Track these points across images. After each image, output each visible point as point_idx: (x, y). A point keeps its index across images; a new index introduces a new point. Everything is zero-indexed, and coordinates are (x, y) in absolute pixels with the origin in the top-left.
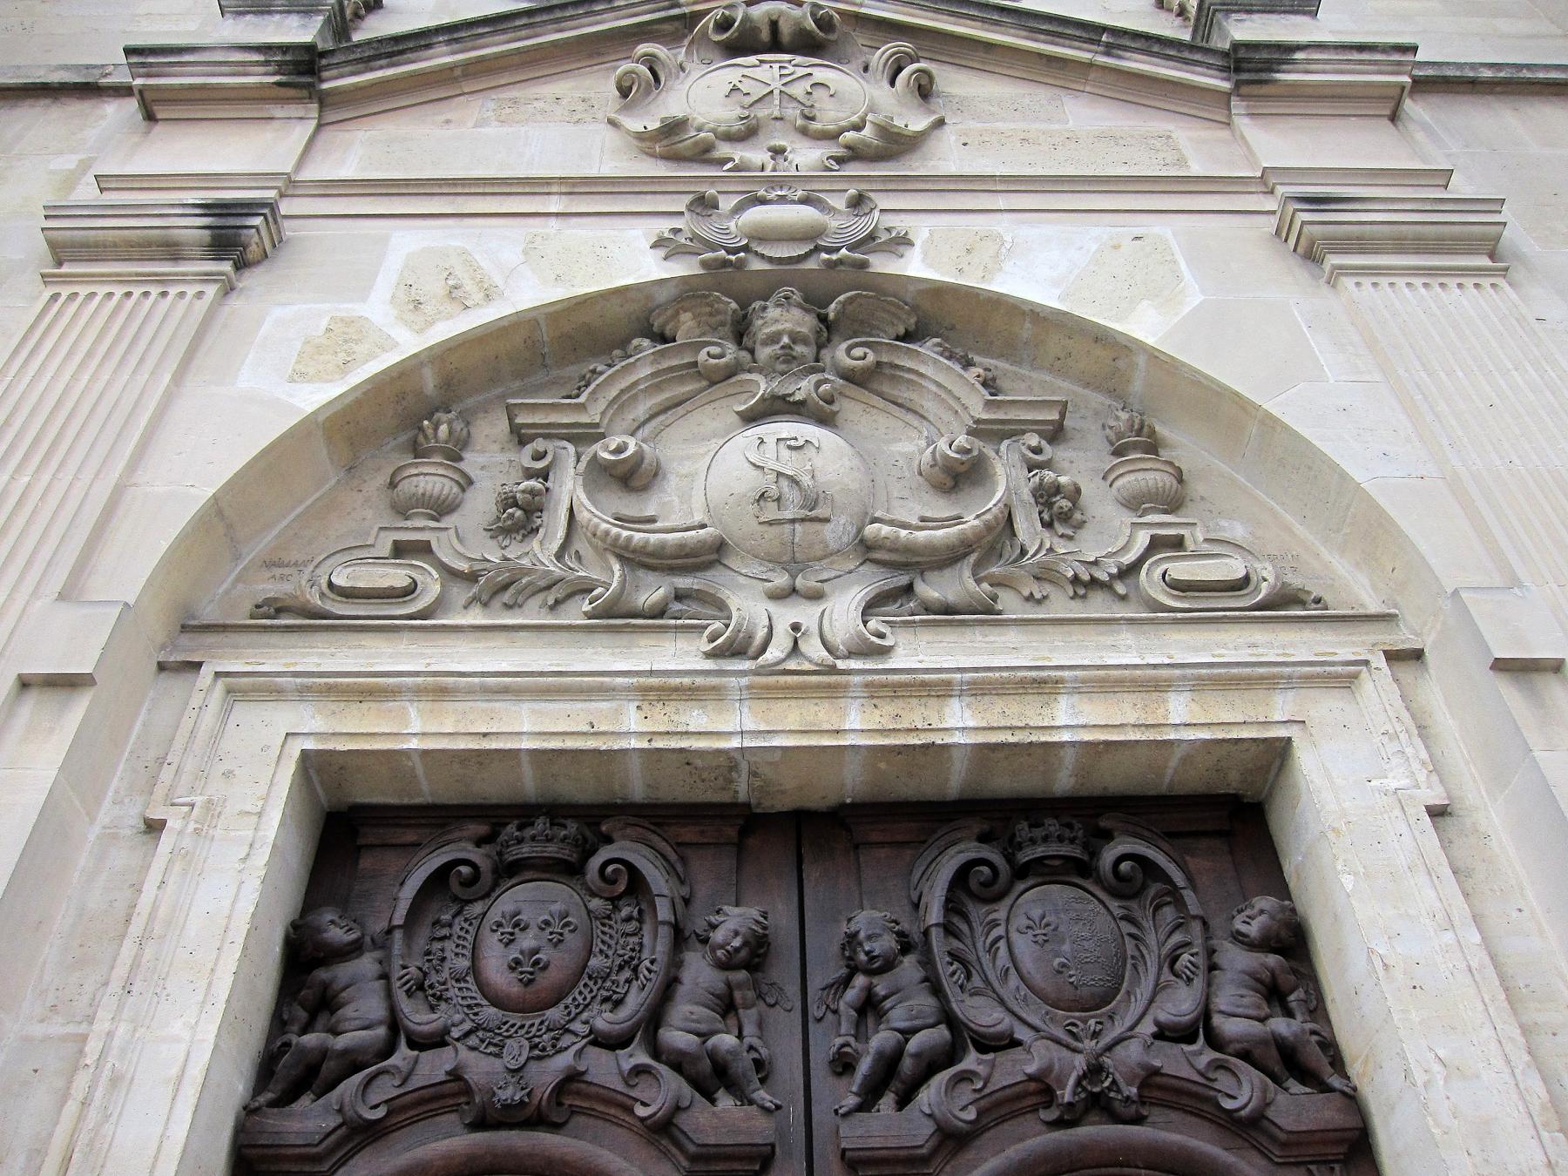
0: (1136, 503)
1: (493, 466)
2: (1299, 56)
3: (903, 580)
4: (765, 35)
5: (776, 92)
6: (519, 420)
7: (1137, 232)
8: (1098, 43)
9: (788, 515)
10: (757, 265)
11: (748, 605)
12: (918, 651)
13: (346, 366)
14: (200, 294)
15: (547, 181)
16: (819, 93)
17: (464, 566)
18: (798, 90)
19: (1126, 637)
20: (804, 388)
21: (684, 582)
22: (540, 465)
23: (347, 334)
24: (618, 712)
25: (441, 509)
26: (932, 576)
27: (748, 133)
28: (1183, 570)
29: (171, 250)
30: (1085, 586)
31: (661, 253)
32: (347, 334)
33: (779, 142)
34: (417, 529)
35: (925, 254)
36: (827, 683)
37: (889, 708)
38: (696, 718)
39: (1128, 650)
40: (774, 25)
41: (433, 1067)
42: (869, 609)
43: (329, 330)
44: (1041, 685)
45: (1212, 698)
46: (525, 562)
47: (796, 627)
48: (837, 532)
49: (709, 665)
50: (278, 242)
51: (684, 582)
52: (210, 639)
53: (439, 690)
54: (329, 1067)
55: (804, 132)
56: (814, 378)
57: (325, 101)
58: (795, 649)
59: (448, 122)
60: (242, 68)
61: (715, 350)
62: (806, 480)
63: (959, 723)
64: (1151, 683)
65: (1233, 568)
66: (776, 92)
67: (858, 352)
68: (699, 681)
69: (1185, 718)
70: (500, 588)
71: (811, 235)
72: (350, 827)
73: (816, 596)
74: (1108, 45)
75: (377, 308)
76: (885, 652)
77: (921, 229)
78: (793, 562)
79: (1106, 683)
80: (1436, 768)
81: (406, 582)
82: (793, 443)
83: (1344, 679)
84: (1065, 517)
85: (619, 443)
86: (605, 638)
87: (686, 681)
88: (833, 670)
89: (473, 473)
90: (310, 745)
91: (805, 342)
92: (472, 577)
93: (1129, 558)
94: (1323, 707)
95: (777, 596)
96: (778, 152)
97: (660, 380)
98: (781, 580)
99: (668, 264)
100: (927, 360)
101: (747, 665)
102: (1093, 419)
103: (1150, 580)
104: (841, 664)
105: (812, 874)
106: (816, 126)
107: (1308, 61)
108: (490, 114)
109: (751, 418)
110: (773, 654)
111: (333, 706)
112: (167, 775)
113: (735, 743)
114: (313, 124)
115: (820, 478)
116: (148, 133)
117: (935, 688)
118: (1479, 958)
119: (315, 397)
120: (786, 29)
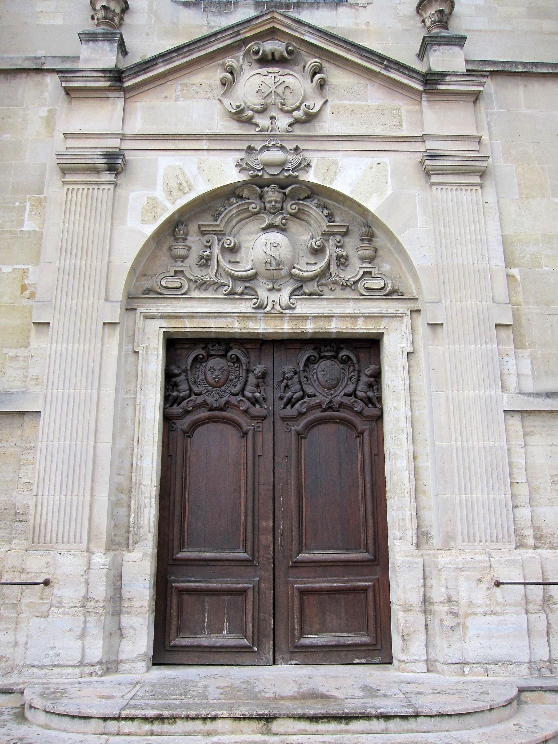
0: (363, 259)
1: (195, 241)
2: (448, 78)
3: (300, 284)
4: (270, 57)
5: (273, 92)
6: (202, 229)
7: (379, 160)
8: (383, 64)
9: (272, 268)
10: (266, 176)
11: (263, 294)
12: (302, 307)
13: (155, 219)
14: (109, 189)
15: (202, 135)
16: (288, 92)
17: (193, 278)
18: (280, 90)
19: (352, 304)
20: (278, 220)
21: (247, 284)
22: (208, 244)
23: (153, 205)
24: (233, 322)
25: (184, 258)
26: (308, 284)
27: (263, 111)
28: (370, 284)
29: (96, 170)
30: (344, 287)
31: (238, 169)
32: (153, 205)
33: (274, 114)
34: (179, 266)
35: (315, 171)
36: (280, 316)
37: (294, 322)
38: (251, 324)
39: (351, 308)
40: (273, 54)
41: (200, 399)
42: (292, 294)
43: (148, 203)
44: (329, 317)
45: (368, 321)
46: (207, 277)
47: (274, 301)
48: (284, 272)
49: (253, 311)
50: (125, 163)
51: (247, 284)
52: (136, 301)
53: (192, 316)
54: (179, 400)
55: (282, 110)
56: (280, 217)
57: (126, 90)
58: (273, 307)
59: (166, 97)
60: (96, 79)
61: (254, 206)
62: (277, 258)
64: (354, 317)
65: (381, 284)
66: (273, 92)
67: (293, 207)
68: (251, 315)
69: (361, 327)
70: (203, 285)
71: (281, 164)
72: (174, 344)
73: (279, 290)
74: (386, 66)
75: (159, 193)
76: (294, 308)
77: (314, 158)
78: (273, 280)
79: (344, 317)
80: (413, 342)
81: (179, 285)
82: (274, 245)
83: (399, 317)
84: (343, 264)
85: (230, 241)
86: (228, 301)
87: (248, 315)
88: (282, 313)
89: (191, 245)
90: (165, 330)
91: (279, 202)
92: (196, 281)
93: (356, 279)
94: (394, 324)
95: (270, 290)
96: (273, 118)
97: (239, 213)
98: (271, 286)
99: (240, 174)
100: (312, 209)
101: (262, 311)
103: (360, 285)
104: (284, 311)
105: (276, 355)
106: (286, 108)
107: (450, 80)
108: (179, 93)
109: (264, 230)
110: (268, 309)
111: (168, 320)
112: (136, 340)
113: (259, 331)
114: (123, 99)
115: (281, 256)
117: (304, 317)
118: (407, 387)
119: (150, 229)
120: (277, 56)
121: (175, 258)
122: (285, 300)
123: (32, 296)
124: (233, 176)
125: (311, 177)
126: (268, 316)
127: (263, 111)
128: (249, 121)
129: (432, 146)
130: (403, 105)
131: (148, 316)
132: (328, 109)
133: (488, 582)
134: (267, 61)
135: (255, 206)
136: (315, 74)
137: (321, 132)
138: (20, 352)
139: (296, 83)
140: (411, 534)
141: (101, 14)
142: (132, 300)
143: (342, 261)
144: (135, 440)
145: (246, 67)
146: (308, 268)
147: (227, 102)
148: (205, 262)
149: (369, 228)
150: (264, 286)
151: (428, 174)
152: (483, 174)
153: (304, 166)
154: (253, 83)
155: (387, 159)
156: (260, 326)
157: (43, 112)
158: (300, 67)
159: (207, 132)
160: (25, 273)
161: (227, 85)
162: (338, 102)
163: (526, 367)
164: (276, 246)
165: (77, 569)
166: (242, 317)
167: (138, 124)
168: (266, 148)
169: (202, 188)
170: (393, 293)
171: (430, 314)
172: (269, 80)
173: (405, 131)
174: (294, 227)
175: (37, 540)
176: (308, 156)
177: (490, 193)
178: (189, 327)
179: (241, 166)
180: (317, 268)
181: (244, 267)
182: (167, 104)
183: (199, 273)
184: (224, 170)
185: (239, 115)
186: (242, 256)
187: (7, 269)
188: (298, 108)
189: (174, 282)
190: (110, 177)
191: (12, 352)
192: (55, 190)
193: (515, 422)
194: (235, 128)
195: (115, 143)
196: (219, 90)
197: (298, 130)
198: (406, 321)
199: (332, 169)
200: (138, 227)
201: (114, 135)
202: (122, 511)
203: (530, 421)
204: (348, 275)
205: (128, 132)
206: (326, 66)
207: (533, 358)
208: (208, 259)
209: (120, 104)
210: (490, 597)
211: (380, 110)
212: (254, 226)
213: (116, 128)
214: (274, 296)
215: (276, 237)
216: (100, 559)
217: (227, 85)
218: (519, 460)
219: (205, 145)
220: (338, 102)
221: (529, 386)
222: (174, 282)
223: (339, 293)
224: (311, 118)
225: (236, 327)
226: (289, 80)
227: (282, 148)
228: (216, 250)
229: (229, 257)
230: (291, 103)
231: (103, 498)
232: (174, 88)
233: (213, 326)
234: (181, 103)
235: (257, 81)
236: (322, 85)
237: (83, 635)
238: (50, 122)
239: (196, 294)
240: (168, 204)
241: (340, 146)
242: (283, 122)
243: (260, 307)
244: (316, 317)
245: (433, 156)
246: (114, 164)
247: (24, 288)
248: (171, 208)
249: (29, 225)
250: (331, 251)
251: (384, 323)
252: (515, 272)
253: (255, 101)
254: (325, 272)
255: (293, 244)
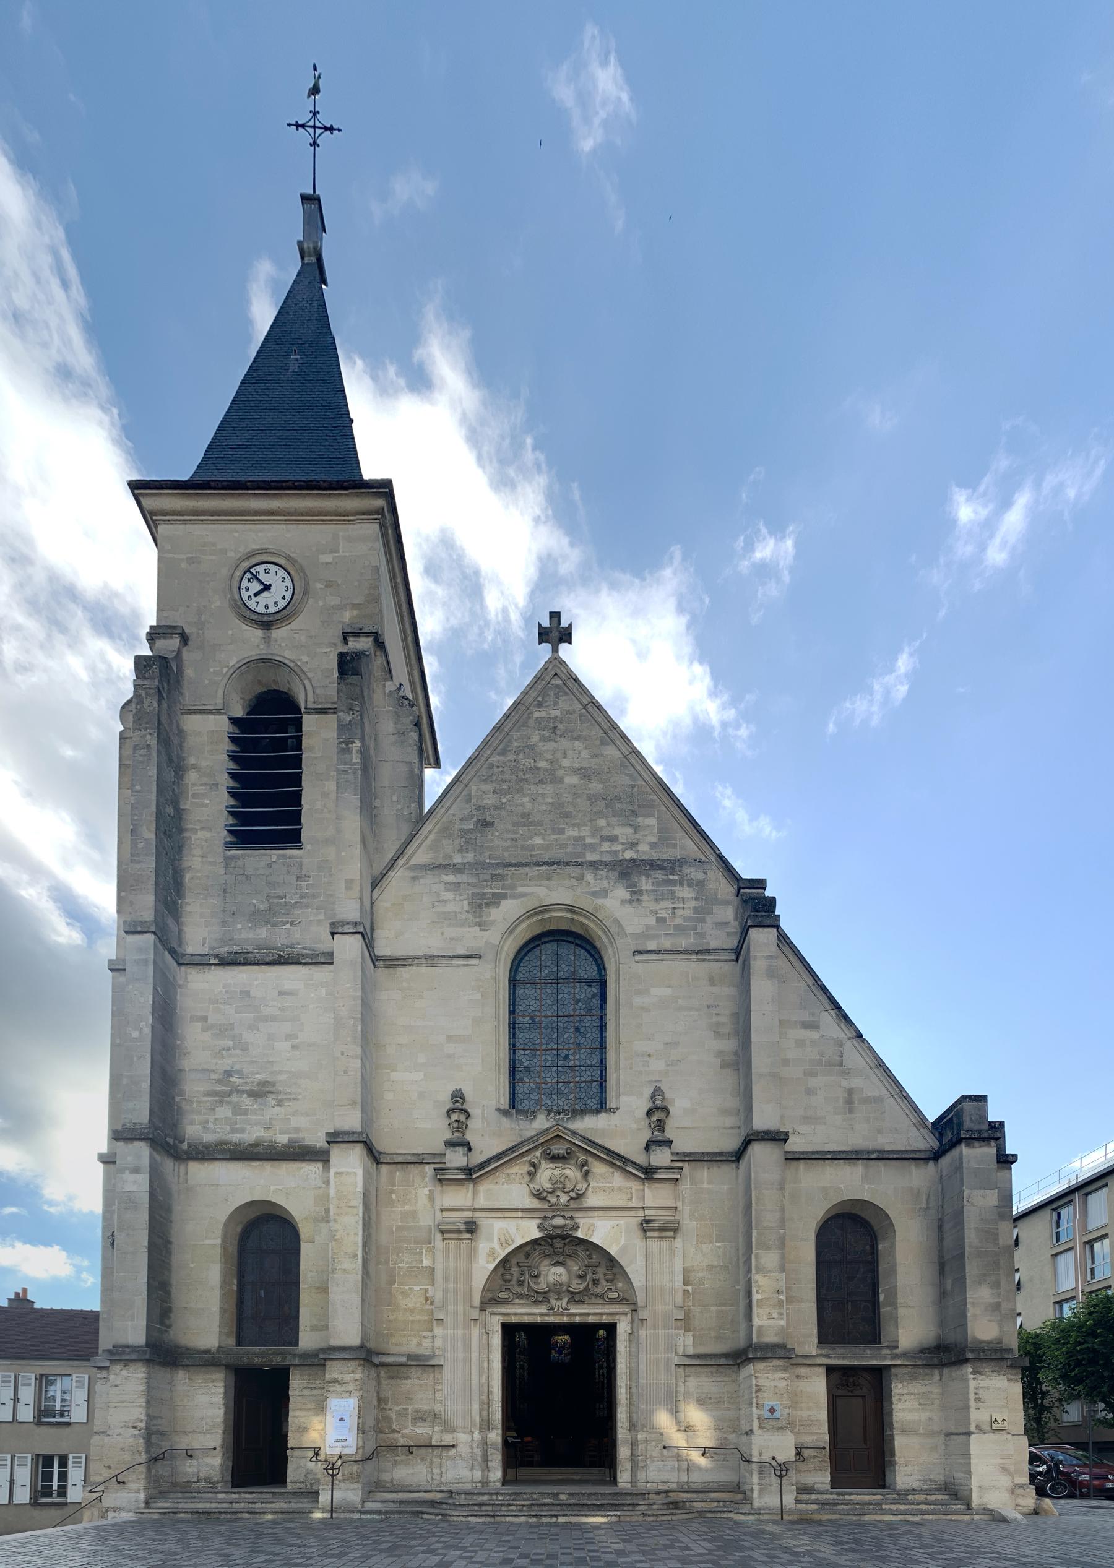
0: (607, 1281)
1: (515, 1270)
11: (553, 1302)
20: (561, 1259)
23: (492, 1253)
25: (510, 1281)
30: (597, 1296)
36: (562, 1314)
44: (588, 1314)
53: (515, 1314)
63: (577, 1319)
64: (602, 1314)
70: (520, 1296)
71: (563, 1227)
75: (496, 1245)
77: (581, 1222)
78: (559, 1293)
83: (626, 1314)
85: (535, 1272)
94: (623, 1317)
102: (604, 1262)
116: (443, 1192)
117: (575, 1314)
119: (492, 1266)
121: (505, 1281)
122: (564, 1305)
123: (432, 1303)
124: (536, 1234)
125: (579, 1234)
126: (555, 1314)
127: (552, 1192)
128: (544, 1199)
129: (650, 1214)
130: (634, 1186)
131: (492, 1314)
132: (590, 1189)
133: (661, 1446)
134: (555, 1158)
135: (549, 1250)
136: (583, 1166)
137: (585, 1205)
138: (429, 1334)
139: (572, 1173)
140: (627, 1425)
141: (455, 1125)
142: (484, 1304)
143: (596, 1282)
144: (489, 1378)
145: (543, 1162)
146: (577, 1286)
147: (532, 1186)
148: (521, 1283)
149: (611, 1263)
150: (556, 1299)
151: (645, 1231)
152: (676, 1230)
153: (576, 1227)
154: (547, 1173)
155: (622, 1222)
156: (551, 1319)
157: (426, 1191)
158: (573, 1162)
159: (521, 1206)
160: (426, 1291)
161: (531, 1175)
162: (595, 1184)
163: (689, 1340)
164: (560, 1275)
165: (466, 1440)
166: (541, 1314)
167: (482, 1202)
168: (554, 1216)
169: (519, 1242)
170: (623, 1300)
171: (642, 1314)
172: (556, 1172)
173: (633, 1205)
174: (569, 1262)
175: (448, 1428)
176: (577, 1220)
177: (678, 1243)
178: (514, 1319)
179: (541, 1228)
180: (582, 1287)
181: (542, 1287)
182: (497, 1187)
183: (518, 1289)
184: (530, 1230)
185: (538, 1195)
186: (541, 1279)
187: (417, 1288)
188: (573, 1190)
189: (505, 1295)
190: (468, 1236)
191: (424, 1334)
192: (438, 1241)
193: (681, 1370)
194: (536, 1203)
195: (469, 1214)
196: (527, 1178)
197: (573, 1205)
198: (629, 1317)
199: (591, 1228)
200: (484, 1266)
201: (469, 1209)
202: (485, 1414)
203: (688, 1369)
204: (598, 1290)
205: (477, 1207)
206: (590, 1160)
207: (694, 1336)
208: (523, 1281)
209: (471, 1187)
210: (662, 1454)
211: (620, 1189)
212: (547, 1262)
213: (469, 1203)
214: (558, 1303)
215: (560, 1270)
216: (477, 1435)
217: (531, 1175)
218: (681, 1389)
219: (520, 1214)
220: (595, 1184)
221: (690, 1351)
222: (505, 1295)
223: (594, 1300)
224: (580, 1196)
225: (539, 1319)
226: (568, 1172)
227: (563, 1217)
228: (527, 1276)
229: (534, 1280)
230: (569, 1186)
231: (476, 1407)
232: (501, 1176)
233: (526, 1319)
234: (505, 1186)
235: (548, 1173)
236: (587, 1172)
237: (472, 1469)
238: (431, 1198)
239: (517, 1301)
240: (500, 1251)
241: (596, 1214)
242: (564, 1199)
243: (552, 1309)
244: (581, 1314)
245: (648, 1221)
246: (471, 1227)
247: (427, 1299)
248: (502, 1254)
249: (426, 1263)
250: (590, 1276)
251: (617, 1317)
252: (689, 1288)
253: (548, 1186)
254: (587, 1289)
255: (569, 1272)
